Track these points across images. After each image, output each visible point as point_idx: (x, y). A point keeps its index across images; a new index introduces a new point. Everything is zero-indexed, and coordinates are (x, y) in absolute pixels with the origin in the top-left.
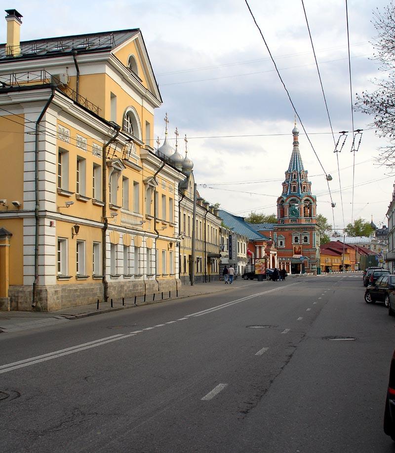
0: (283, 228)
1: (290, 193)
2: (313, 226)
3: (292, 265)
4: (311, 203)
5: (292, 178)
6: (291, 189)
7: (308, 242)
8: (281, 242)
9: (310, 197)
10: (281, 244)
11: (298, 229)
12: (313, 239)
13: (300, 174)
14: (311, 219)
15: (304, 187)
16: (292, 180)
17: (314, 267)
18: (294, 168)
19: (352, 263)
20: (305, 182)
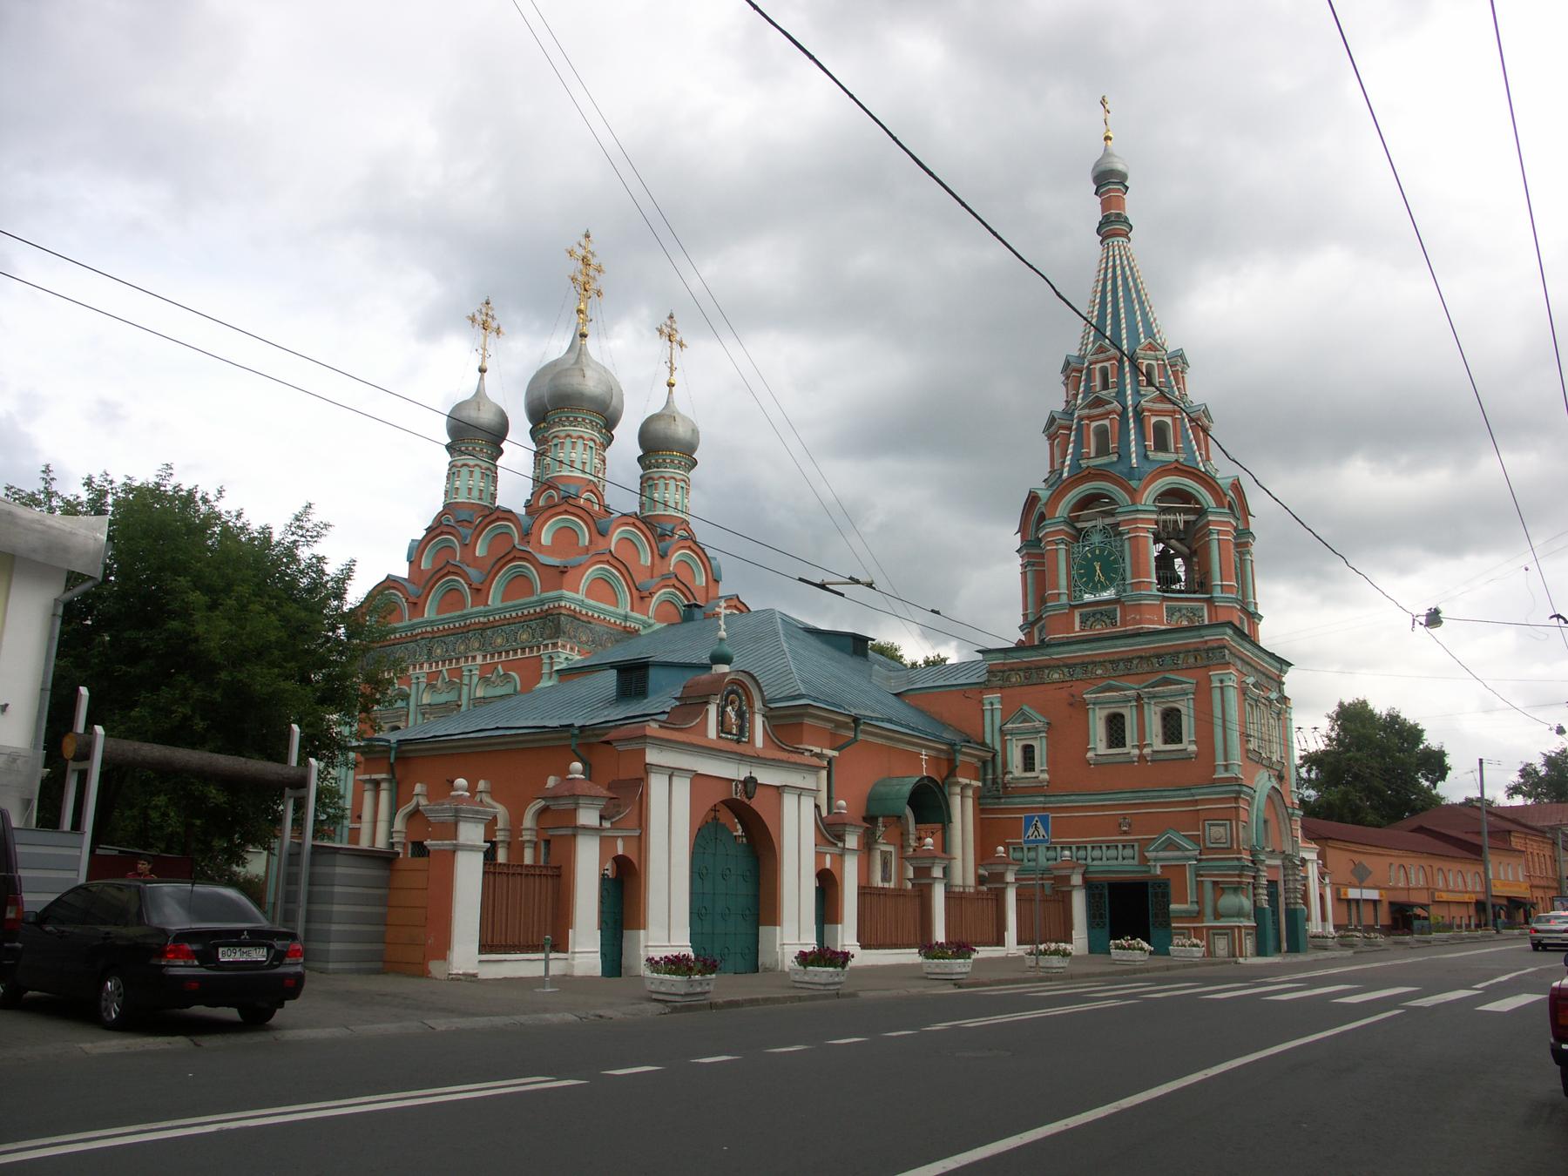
0: (1039, 668)
2: (1211, 637)
3: (1090, 886)
4: (1201, 512)
5: (1088, 389)
6: (1080, 443)
7: (1189, 745)
8: (1028, 752)
9: (1207, 480)
10: (1029, 763)
11: (1124, 666)
12: (1217, 712)
14: (1210, 601)
15: (1160, 430)
17: (1229, 901)
19: (1539, 893)
20: (1163, 397)
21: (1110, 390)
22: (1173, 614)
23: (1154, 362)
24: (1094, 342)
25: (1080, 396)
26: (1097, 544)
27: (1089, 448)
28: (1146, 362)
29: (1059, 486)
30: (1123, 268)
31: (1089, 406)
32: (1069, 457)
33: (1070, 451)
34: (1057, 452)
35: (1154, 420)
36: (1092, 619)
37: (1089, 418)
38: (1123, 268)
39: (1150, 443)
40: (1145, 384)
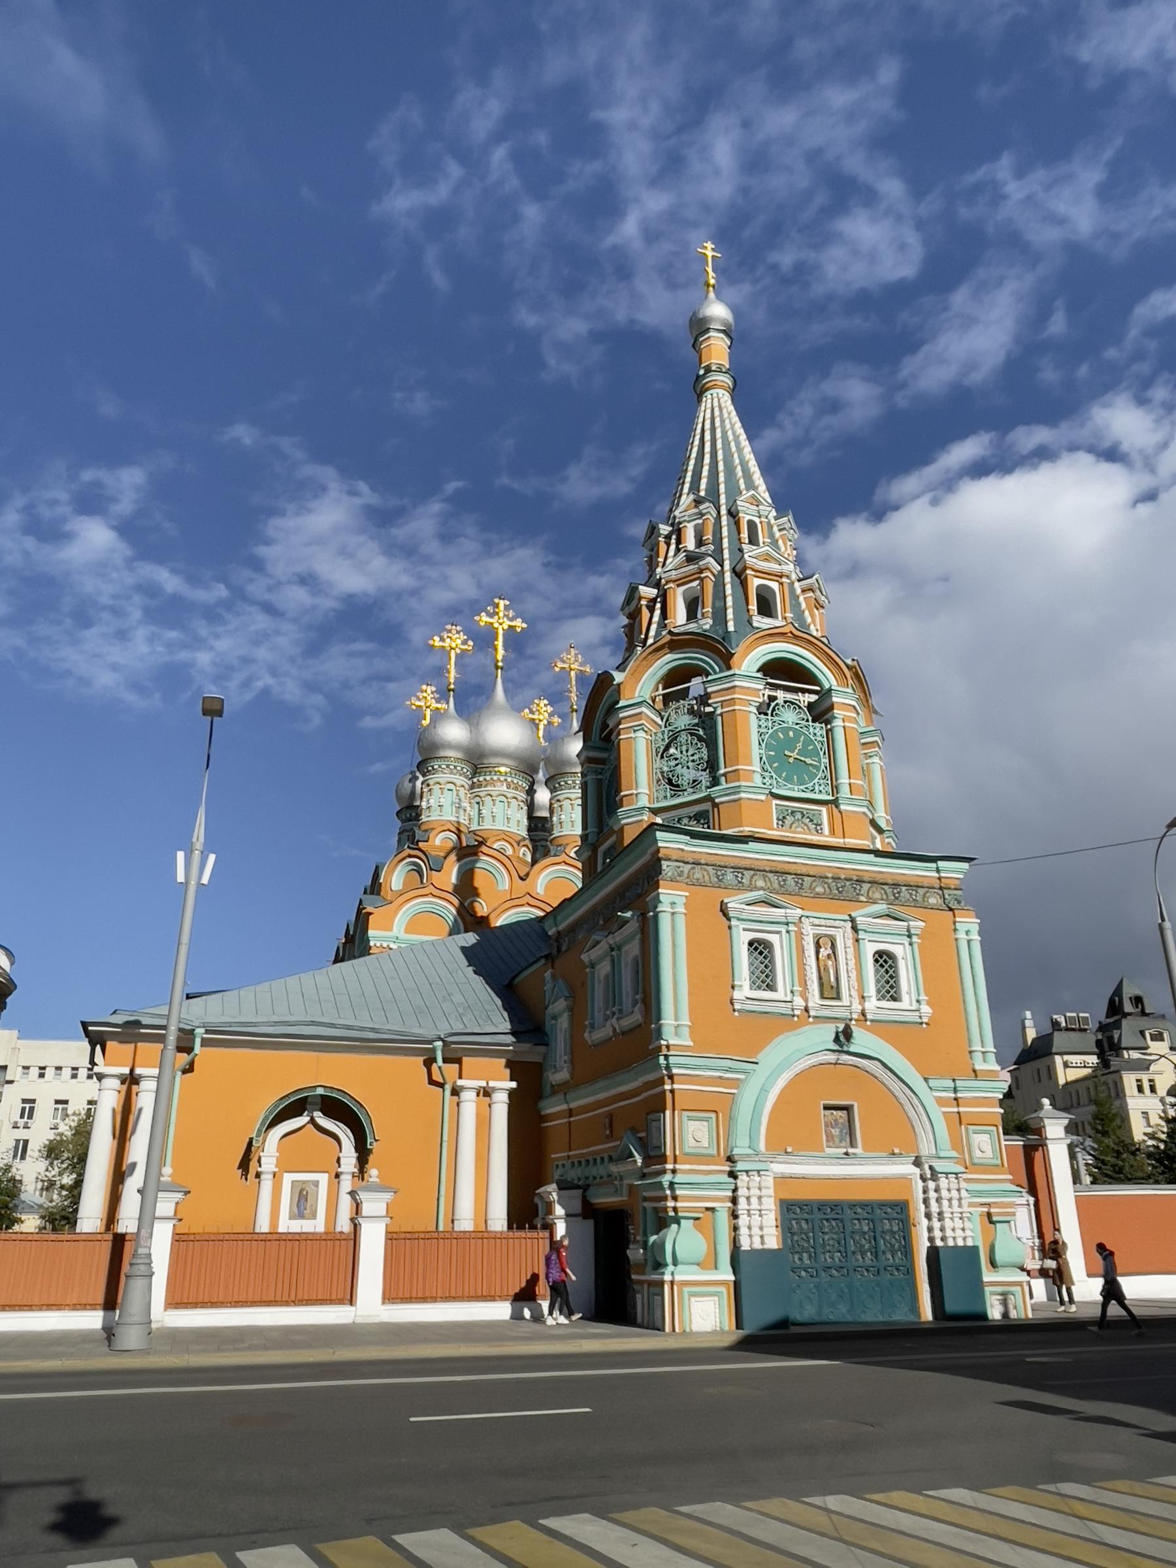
13: (733, 514)
20: (767, 558)
23: (757, 520)
26: (683, 727)
28: (748, 517)
30: (722, 421)
38: (722, 421)
39: (753, 607)
40: (747, 541)
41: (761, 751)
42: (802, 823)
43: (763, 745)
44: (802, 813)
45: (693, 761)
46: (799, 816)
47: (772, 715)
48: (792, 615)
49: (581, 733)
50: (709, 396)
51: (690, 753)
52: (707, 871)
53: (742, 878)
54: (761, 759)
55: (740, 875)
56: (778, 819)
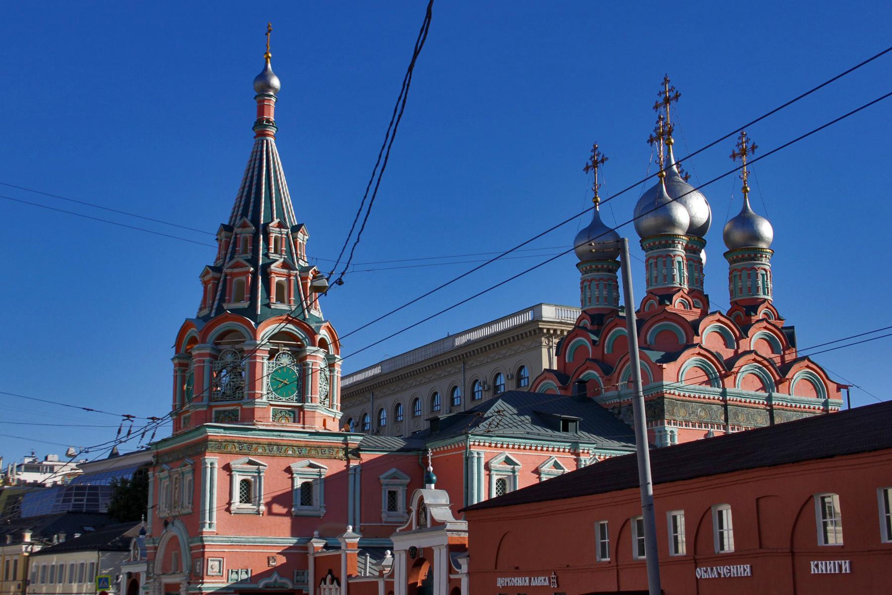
1: (220, 310)
4: (302, 347)
16: (232, 258)
18: (245, 214)
21: (247, 255)
22: (276, 415)
24: (241, 219)
25: (228, 256)
26: (229, 363)
27: (230, 296)
29: (206, 321)
31: (232, 267)
32: (216, 303)
33: (217, 297)
34: (210, 296)
35: (277, 279)
36: (222, 415)
37: (232, 275)
40: (273, 251)
41: (268, 380)
42: (286, 417)
43: (270, 377)
44: (286, 412)
45: (233, 382)
46: (283, 413)
47: (276, 361)
48: (294, 299)
49: (175, 347)
50: (260, 141)
51: (232, 377)
52: (234, 445)
53: (251, 449)
54: (268, 384)
55: (250, 447)
56: (273, 416)
